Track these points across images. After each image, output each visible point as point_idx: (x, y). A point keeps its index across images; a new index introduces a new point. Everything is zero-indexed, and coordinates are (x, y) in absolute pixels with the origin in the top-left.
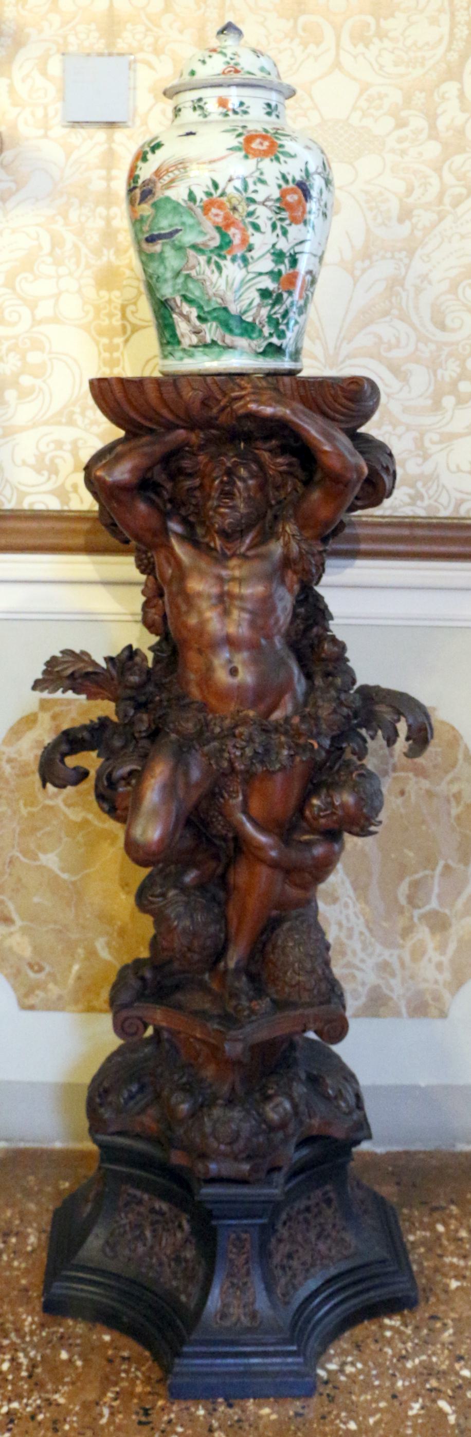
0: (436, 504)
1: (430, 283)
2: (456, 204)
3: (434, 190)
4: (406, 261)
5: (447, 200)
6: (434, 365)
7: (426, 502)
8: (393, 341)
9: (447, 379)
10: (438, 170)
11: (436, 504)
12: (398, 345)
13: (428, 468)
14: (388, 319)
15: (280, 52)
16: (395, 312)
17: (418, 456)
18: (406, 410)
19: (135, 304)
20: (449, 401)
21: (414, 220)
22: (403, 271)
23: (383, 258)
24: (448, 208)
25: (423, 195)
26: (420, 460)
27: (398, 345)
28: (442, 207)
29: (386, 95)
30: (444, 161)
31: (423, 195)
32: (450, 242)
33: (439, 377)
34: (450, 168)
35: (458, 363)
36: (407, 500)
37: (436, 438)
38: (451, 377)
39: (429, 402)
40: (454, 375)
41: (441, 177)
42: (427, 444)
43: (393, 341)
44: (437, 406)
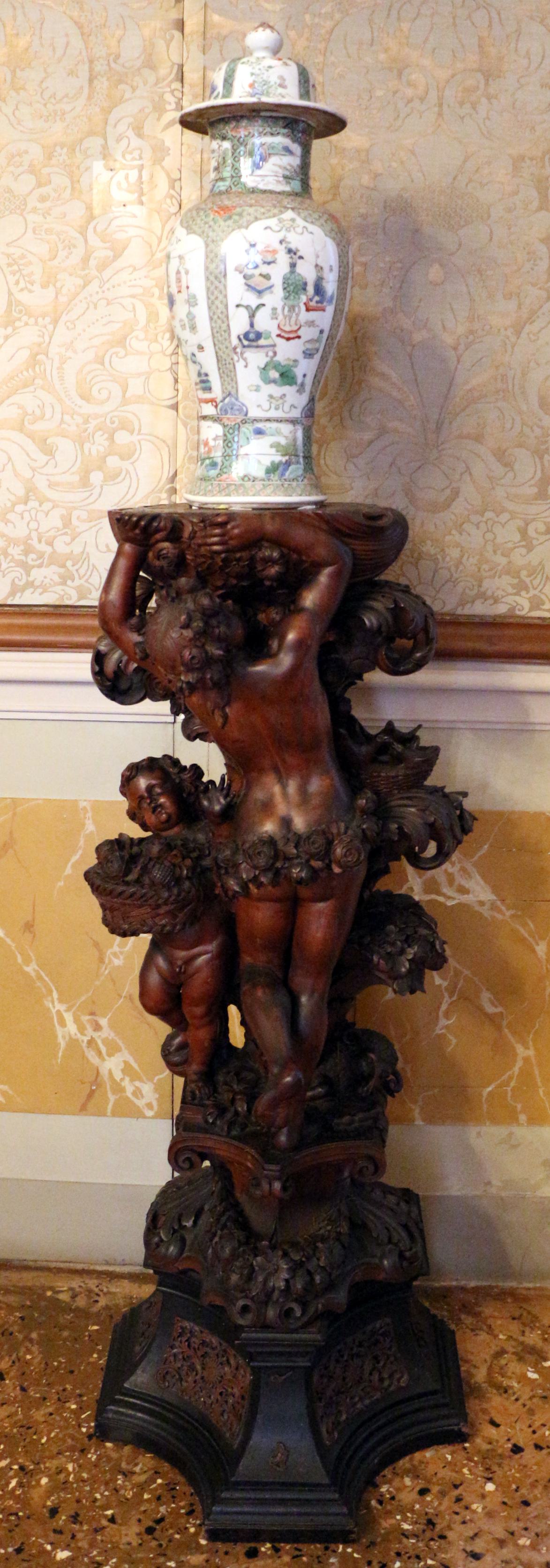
0: (87, 585)
1: (75, 352)
2: (103, 266)
3: (80, 251)
4: (50, 327)
5: (92, 263)
6: (81, 440)
7: (77, 582)
8: (38, 412)
9: (94, 452)
10: (83, 232)
11: (87, 585)
12: (42, 417)
13: (77, 548)
14: (32, 389)
16: (38, 381)
17: (65, 534)
18: (51, 485)
20: (96, 477)
21: (58, 285)
22: (47, 339)
23: (26, 324)
24: (94, 272)
25: (67, 257)
26: (67, 539)
27: (42, 417)
28: (87, 271)
29: (26, 152)
30: (89, 222)
31: (67, 257)
32: (95, 308)
33: (86, 451)
34: (95, 228)
35: (106, 436)
36: (56, 579)
37: (84, 515)
38: (98, 451)
39: (76, 478)
40: (102, 449)
41: (86, 241)
42: (74, 521)
43: (38, 412)
44: (85, 482)
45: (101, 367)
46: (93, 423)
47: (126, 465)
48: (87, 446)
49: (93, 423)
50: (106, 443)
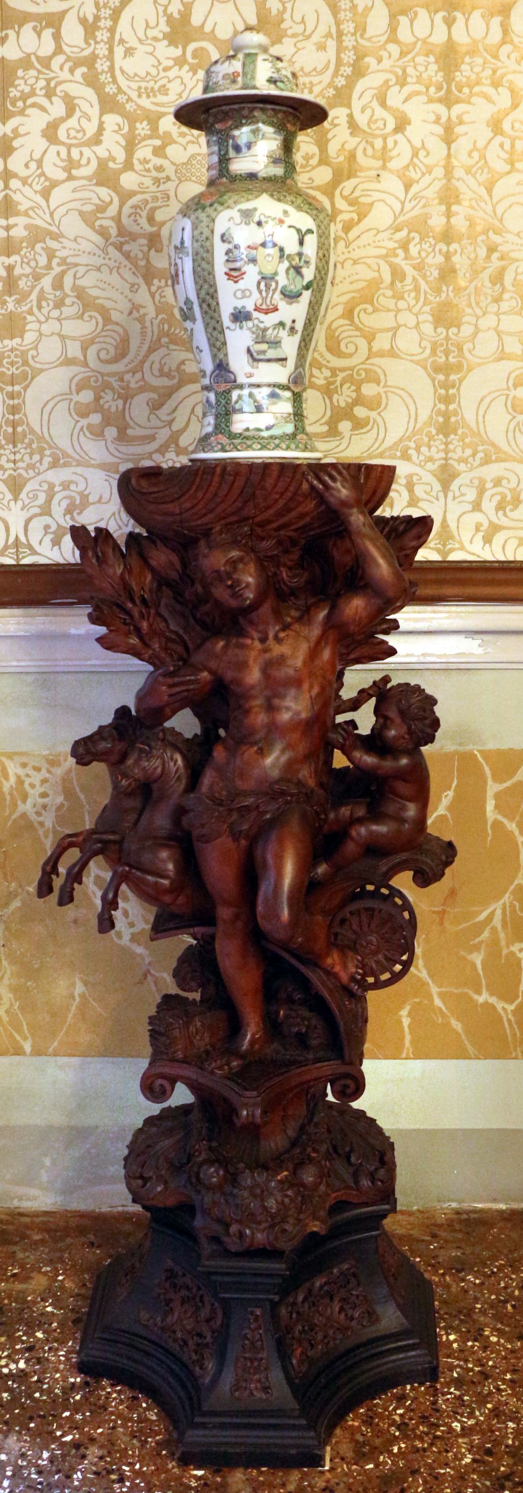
15: (169, 81)
19: (36, 348)
20: (345, 426)
33: (335, 400)
35: (353, 388)
45: (348, 322)
46: (341, 375)
47: (373, 414)
48: (335, 397)
49: (341, 375)
50: (354, 395)
